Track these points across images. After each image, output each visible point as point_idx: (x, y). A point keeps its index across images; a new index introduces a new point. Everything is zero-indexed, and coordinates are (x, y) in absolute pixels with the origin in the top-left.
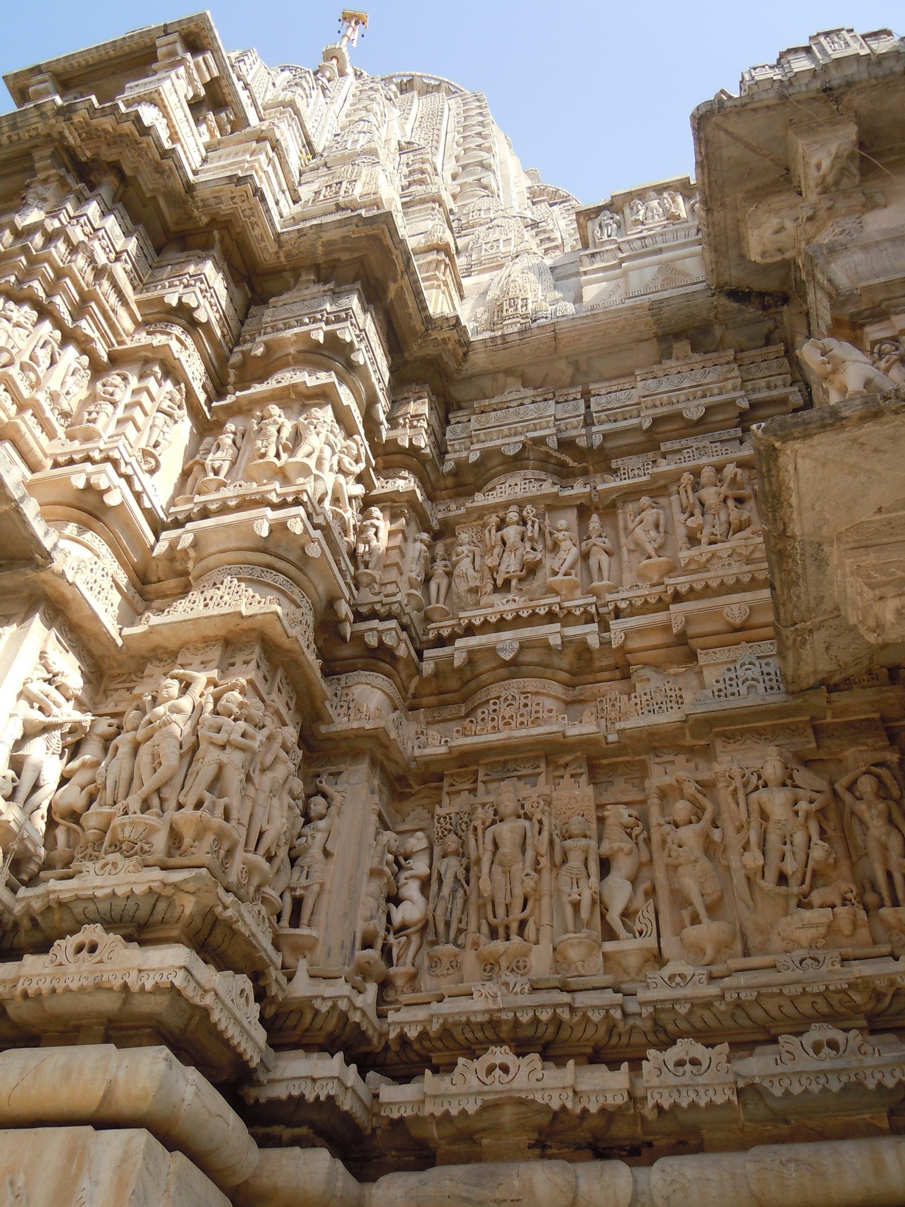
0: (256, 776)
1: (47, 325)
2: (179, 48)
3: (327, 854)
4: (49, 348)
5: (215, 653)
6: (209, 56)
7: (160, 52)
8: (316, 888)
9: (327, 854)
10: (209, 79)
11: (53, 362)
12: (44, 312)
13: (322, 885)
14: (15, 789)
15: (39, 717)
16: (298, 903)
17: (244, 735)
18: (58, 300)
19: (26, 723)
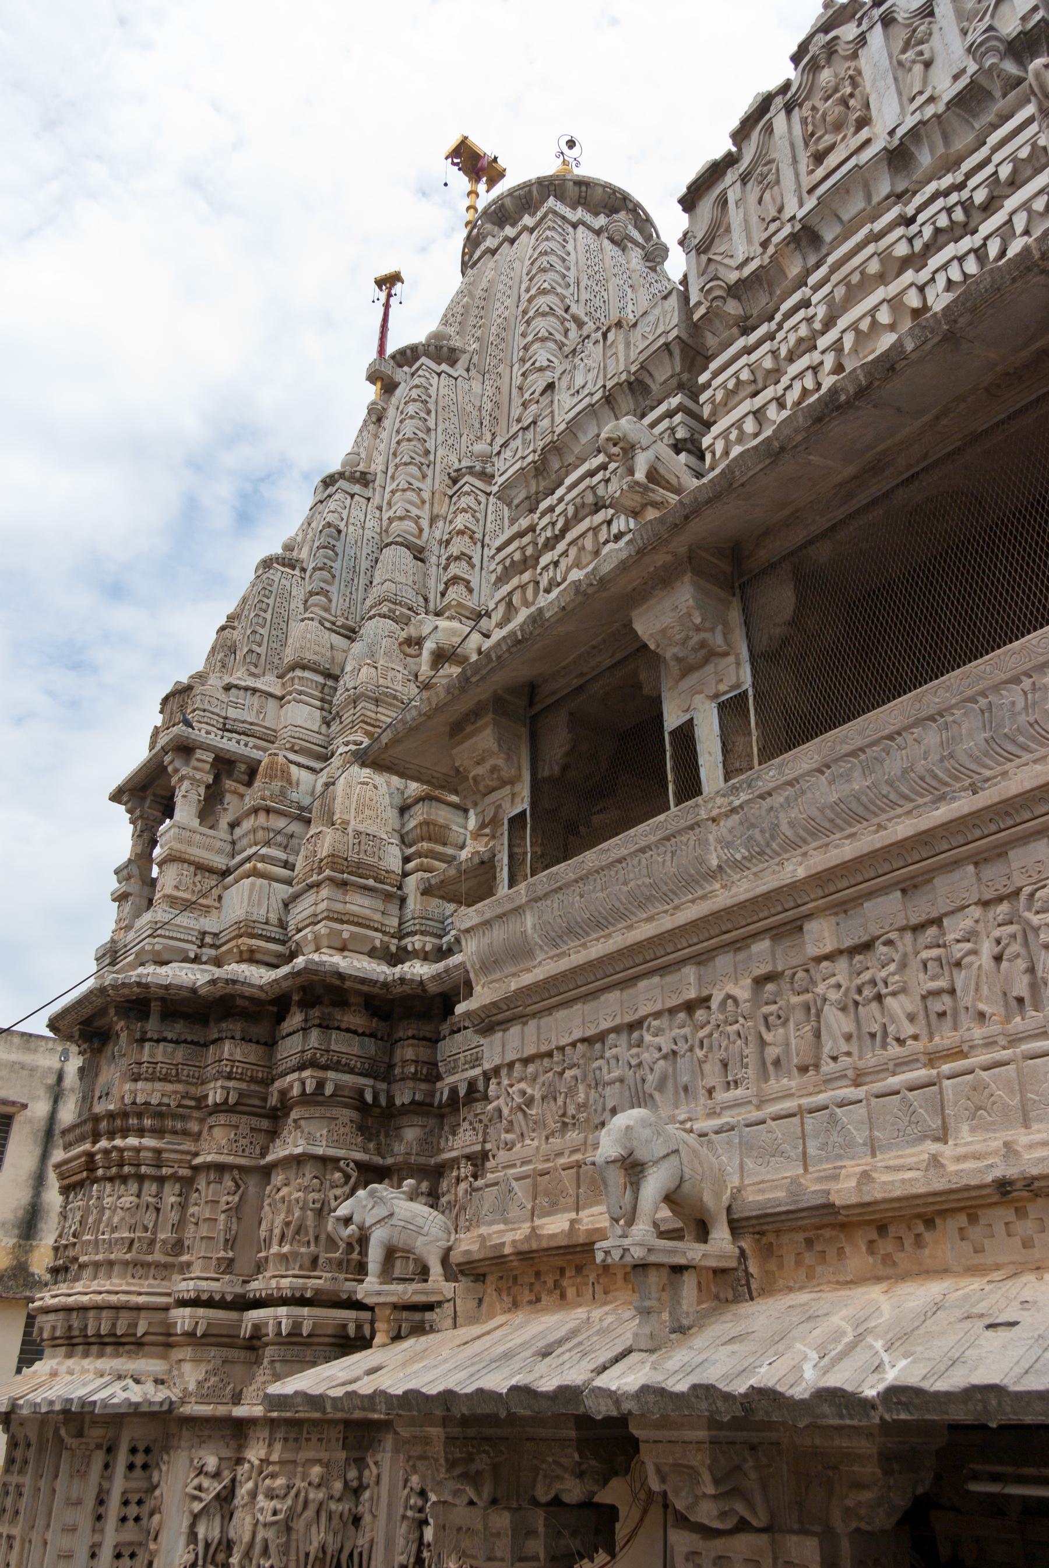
0: (293, 1525)
1: (146, 1185)
2: (177, 764)
3: (374, 1516)
4: (151, 1208)
5: (266, 1434)
6: (199, 754)
7: (170, 769)
8: (366, 1546)
9: (374, 1516)
10: (208, 767)
11: (158, 1210)
12: (141, 1178)
13: (372, 1541)
14: (197, 1555)
15: (197, 1507)
16: (361, 1554)
17: (275, 1513)
18: (143, 1169)
19: (191, 1512)
